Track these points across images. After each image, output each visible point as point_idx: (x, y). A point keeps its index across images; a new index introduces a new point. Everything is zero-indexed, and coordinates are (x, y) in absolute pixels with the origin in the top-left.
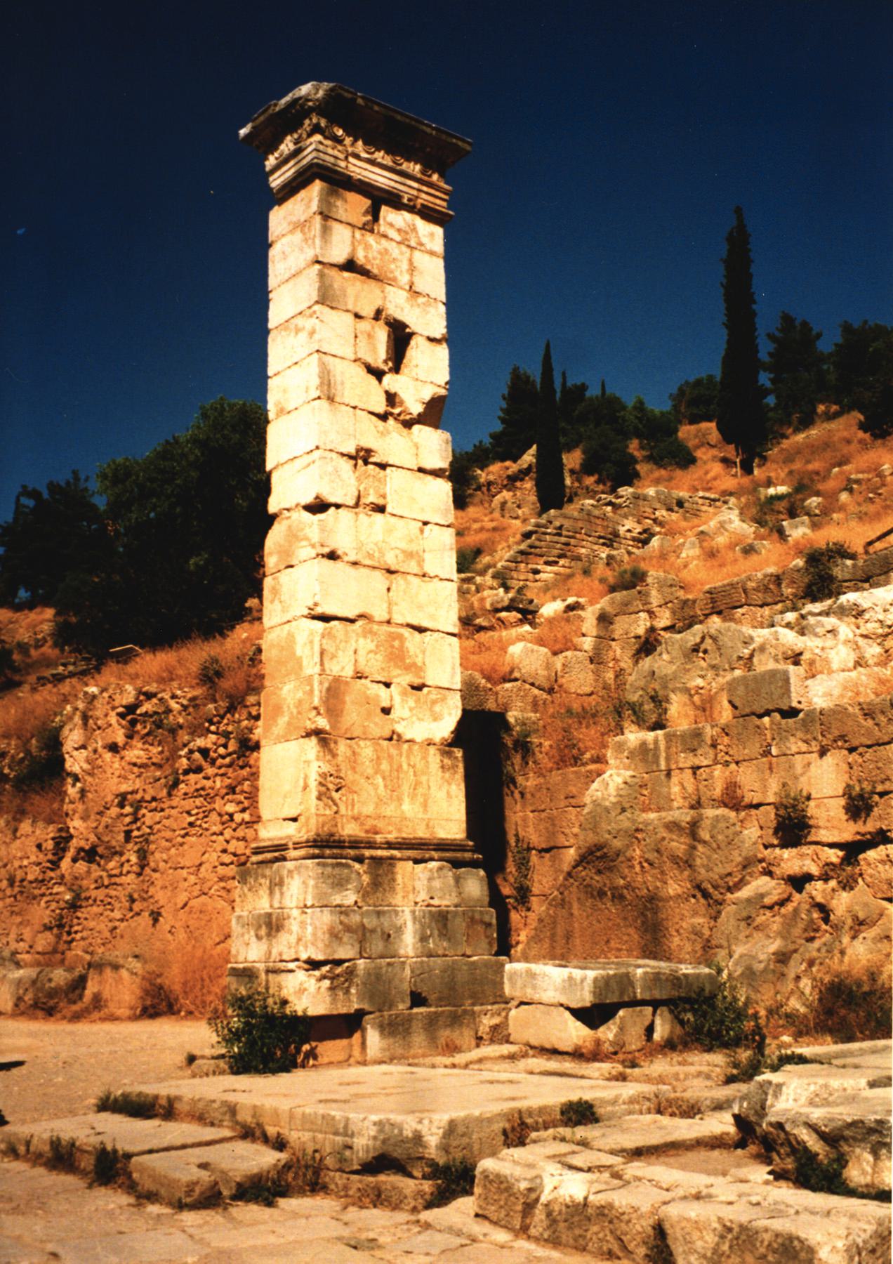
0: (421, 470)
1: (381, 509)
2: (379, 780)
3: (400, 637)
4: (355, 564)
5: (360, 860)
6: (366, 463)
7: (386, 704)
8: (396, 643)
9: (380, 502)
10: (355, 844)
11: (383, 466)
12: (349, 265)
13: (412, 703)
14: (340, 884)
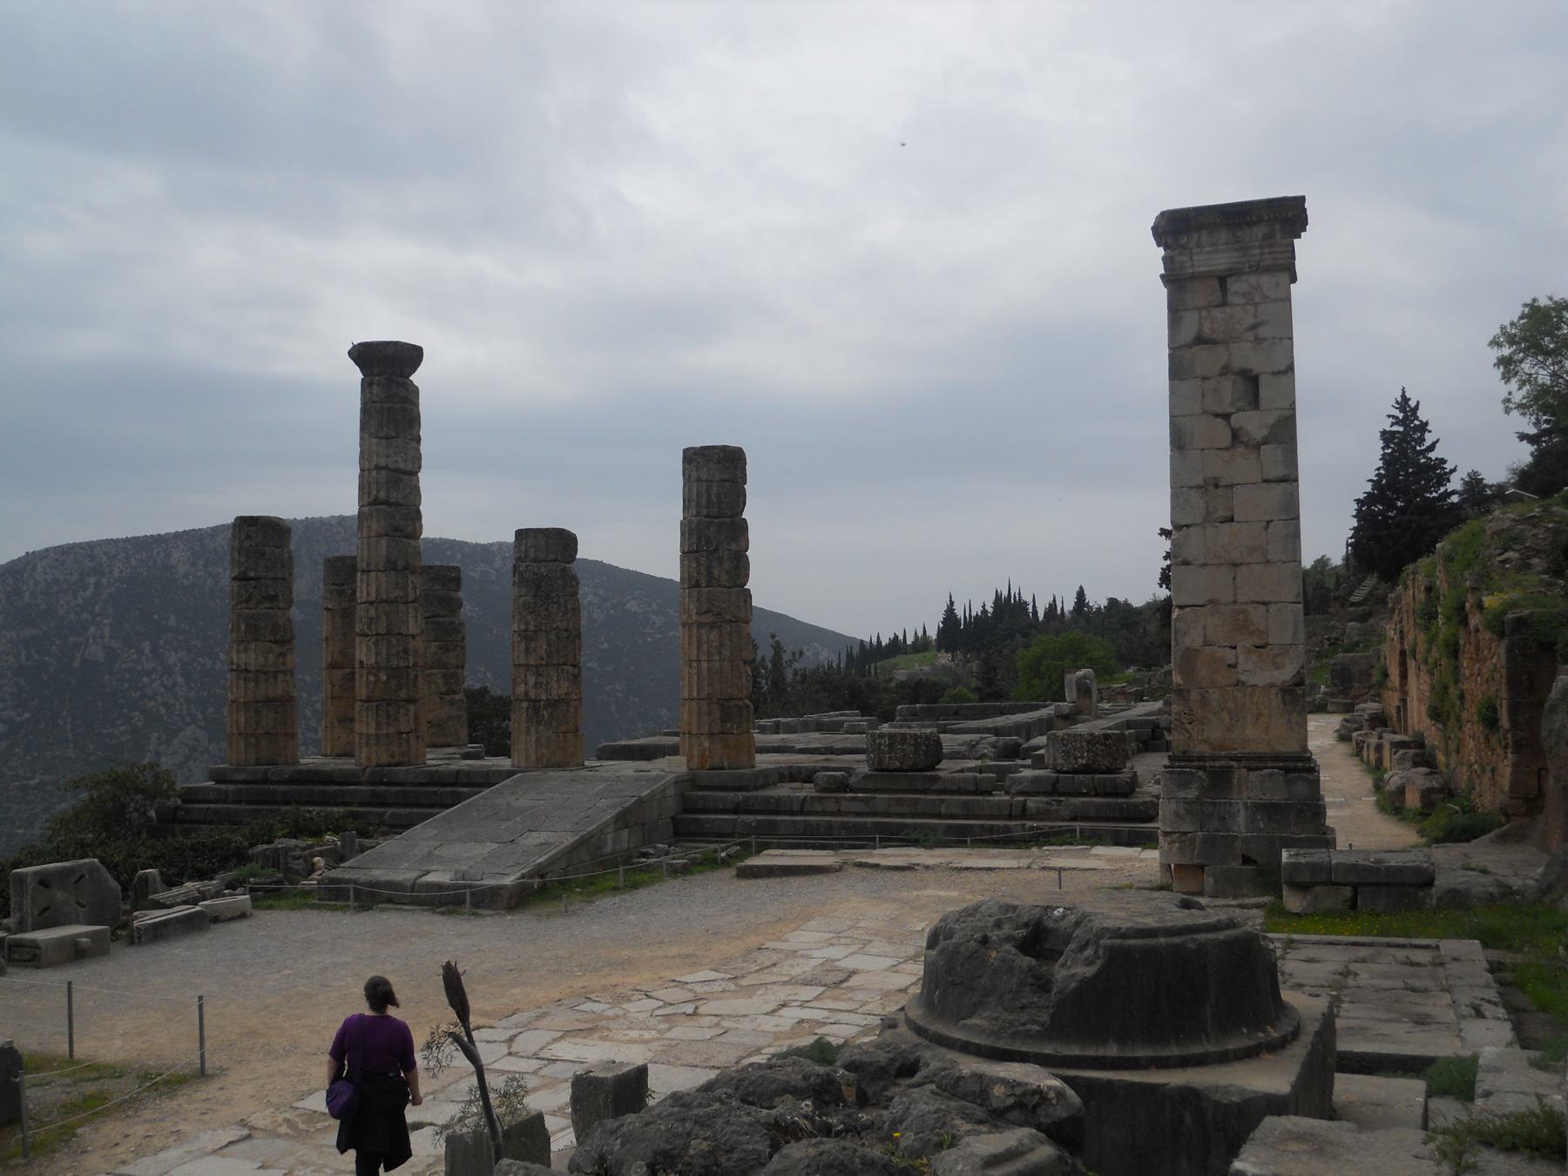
0: (1265, 481)
1: (1231, 520)
2: (1225, 715)
3: (1245, 612)
4: (1204, 565)
5: (1203, 768)
6: (1217, 486)
7: (1232, 661)
8: (1241, 617)
9: (1228, 514)
10: (1201, 758)
11: (1231, 486)
12: (1200, 340)
13: (1254, 658)
14: (1184, 785)
